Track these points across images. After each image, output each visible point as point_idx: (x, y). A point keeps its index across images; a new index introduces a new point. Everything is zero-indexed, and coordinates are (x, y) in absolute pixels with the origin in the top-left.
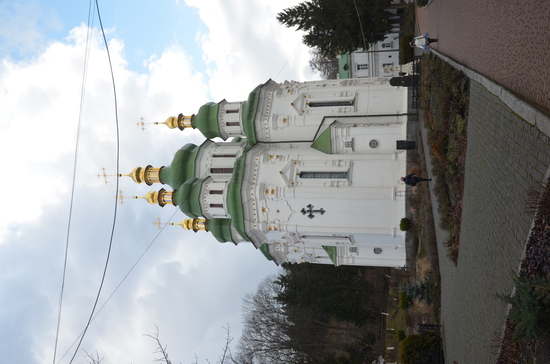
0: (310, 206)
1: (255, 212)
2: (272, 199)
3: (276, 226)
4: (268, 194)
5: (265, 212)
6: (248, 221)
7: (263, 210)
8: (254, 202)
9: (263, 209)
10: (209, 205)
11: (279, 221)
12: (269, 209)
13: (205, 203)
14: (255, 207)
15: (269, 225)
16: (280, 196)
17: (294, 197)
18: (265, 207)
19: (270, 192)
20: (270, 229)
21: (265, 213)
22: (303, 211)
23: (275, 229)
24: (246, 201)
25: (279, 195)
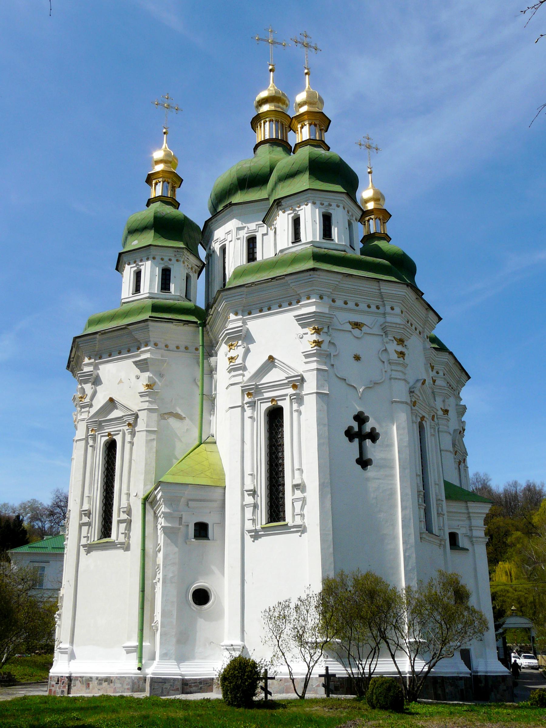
0: (373, 436)
1: (351, 305)
2: (386, 350)
3: (325, 346)
4: (395, 342)
5: (351, 327)
6: (337, 283)
7: (357, 325)
8: (373, 308)
9: (359, 325)
10: (330, 211)
11: (334, 355)
12: (357, 338)
13: (334, 205)
14: (363, 306)
15: (325, 330)
16: (392, 370)
17: (393, 402)
18: (364, 329)
19: (400, 348)
20: (317, 331)
21: (349, 327)
22: (361, 419)
23: (318, 343)
24: (382, 291)
25: (394, 367)
